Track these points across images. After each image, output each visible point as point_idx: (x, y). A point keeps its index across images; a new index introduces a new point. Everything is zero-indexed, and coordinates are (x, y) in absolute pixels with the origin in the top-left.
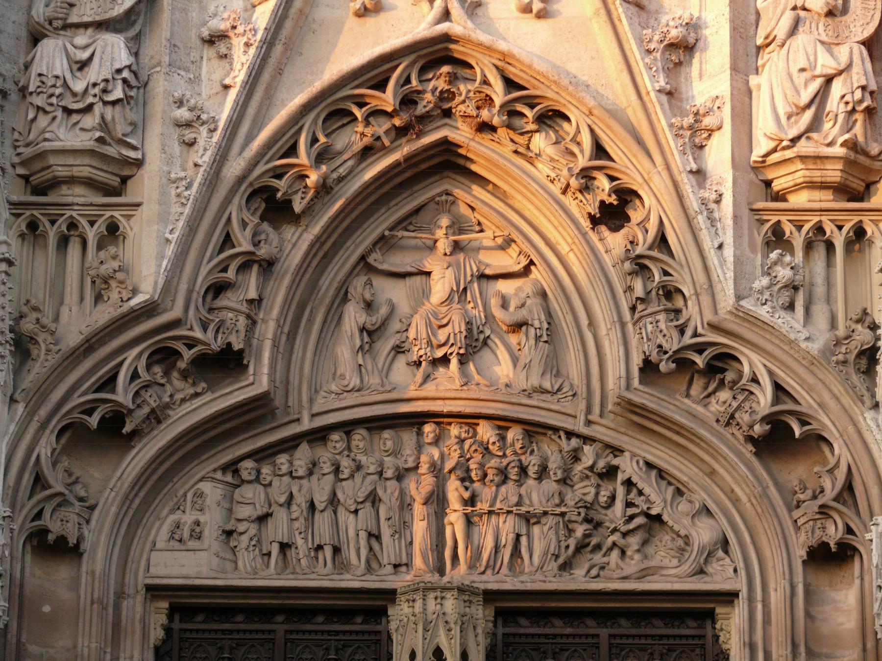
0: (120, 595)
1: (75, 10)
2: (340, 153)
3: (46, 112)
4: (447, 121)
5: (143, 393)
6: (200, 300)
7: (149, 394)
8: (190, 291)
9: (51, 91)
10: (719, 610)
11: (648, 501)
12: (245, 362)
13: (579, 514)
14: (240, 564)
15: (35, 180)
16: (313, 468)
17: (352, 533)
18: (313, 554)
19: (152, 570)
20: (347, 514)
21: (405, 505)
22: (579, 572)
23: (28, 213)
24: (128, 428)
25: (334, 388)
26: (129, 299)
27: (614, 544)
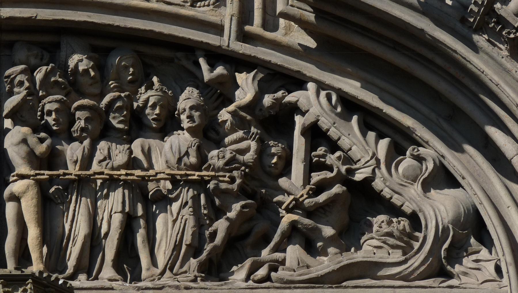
11: (348, 160)
13: (233, 180)
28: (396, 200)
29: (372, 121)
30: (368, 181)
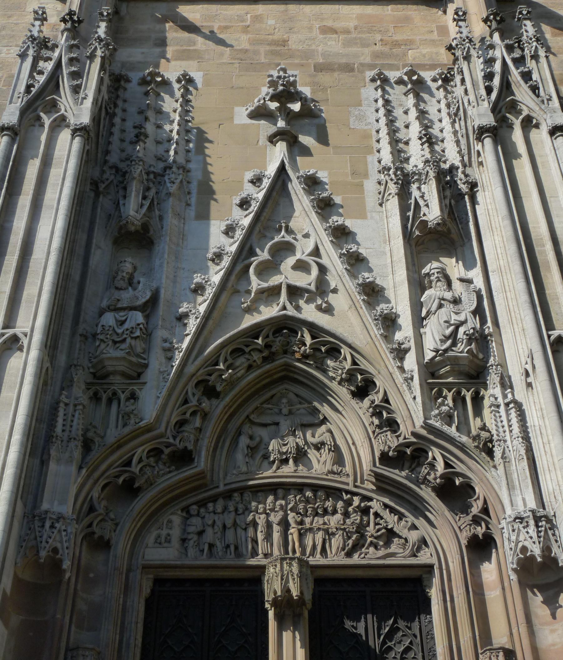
0: (129, 570)
1: (120, 302)
2: (238, 367)
3: (105, 342)
4: (285, 355)
5: (144, 469)
6: (173, 427)
8: (168, 423)
9: (107, 332)
10: (424, 576)
11: (386, 522)
12: (193, 456)
13: (353, 528)
14: (189, 554)
15: (98, 375)
16: (225, 509)
17: (243, 539)
18: (224, 550)
19: (146, 557)
20: (241, 530)
21: (269, 525)
22: (356, 556)
23: (94, 388)
24: (136, 485)
25: (235, 472)
26: (139, 422)
27: (371, 542)
28: (401, 534)
29: (393, 511)
30: (392, 529)
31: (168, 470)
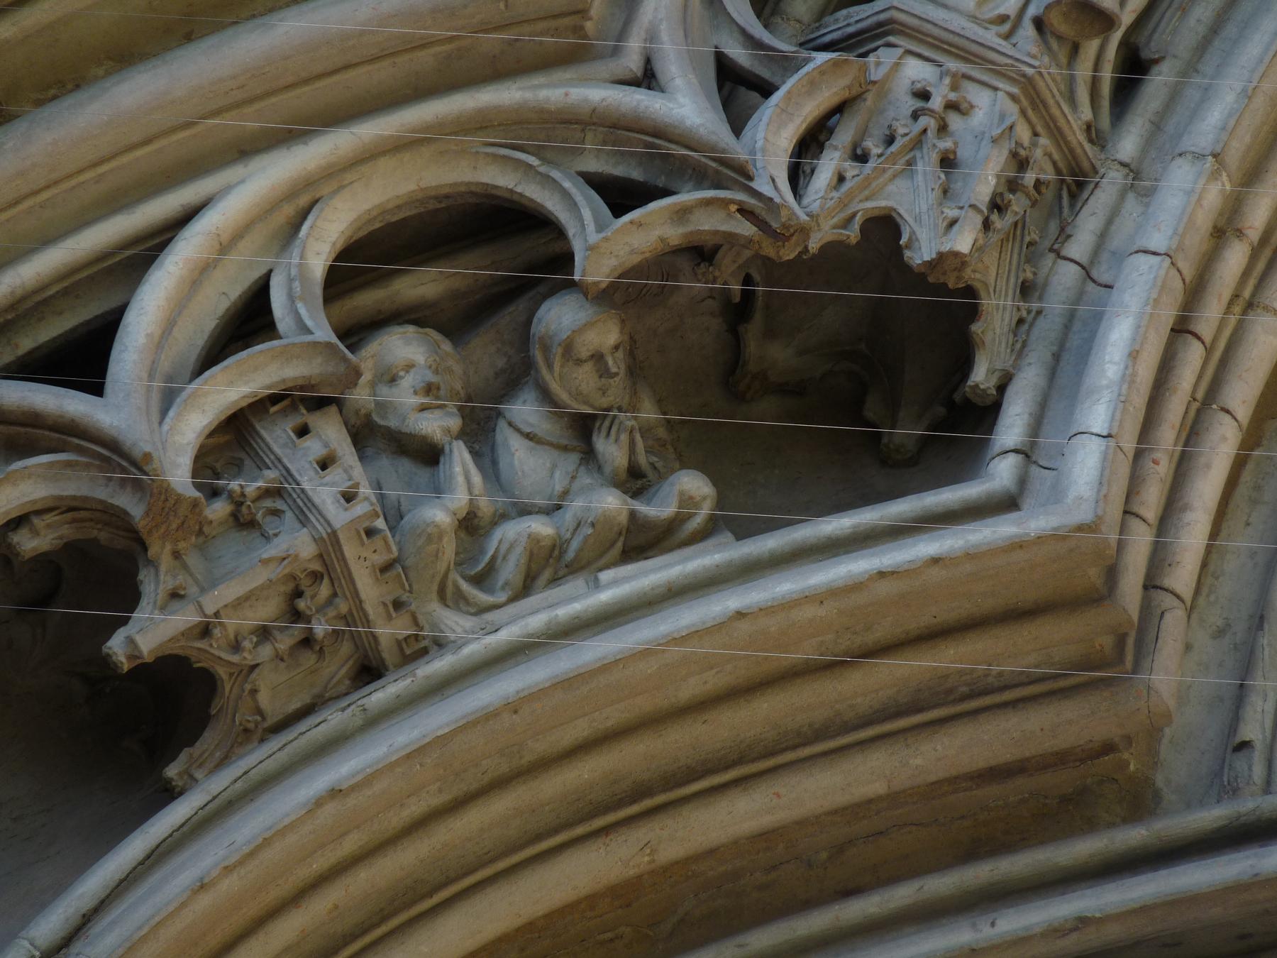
5: (274, 432)
7: (313, 447)
12: (981, 375)
24: (148, 632)
31: (611, 502)
